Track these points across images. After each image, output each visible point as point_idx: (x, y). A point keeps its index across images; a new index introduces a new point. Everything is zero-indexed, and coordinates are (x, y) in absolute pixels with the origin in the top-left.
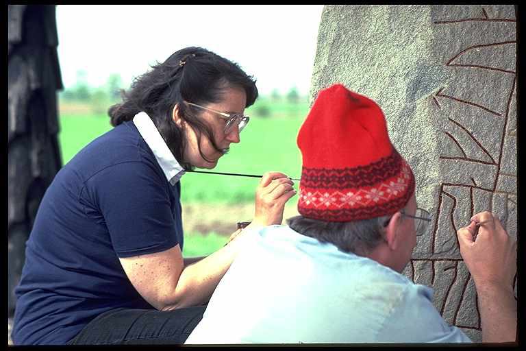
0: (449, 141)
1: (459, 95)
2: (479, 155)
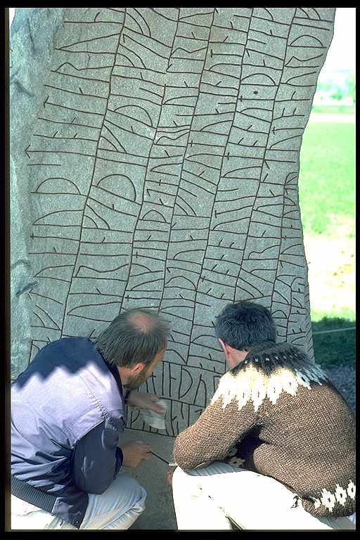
1: (41, 293)
2: (51, 325)
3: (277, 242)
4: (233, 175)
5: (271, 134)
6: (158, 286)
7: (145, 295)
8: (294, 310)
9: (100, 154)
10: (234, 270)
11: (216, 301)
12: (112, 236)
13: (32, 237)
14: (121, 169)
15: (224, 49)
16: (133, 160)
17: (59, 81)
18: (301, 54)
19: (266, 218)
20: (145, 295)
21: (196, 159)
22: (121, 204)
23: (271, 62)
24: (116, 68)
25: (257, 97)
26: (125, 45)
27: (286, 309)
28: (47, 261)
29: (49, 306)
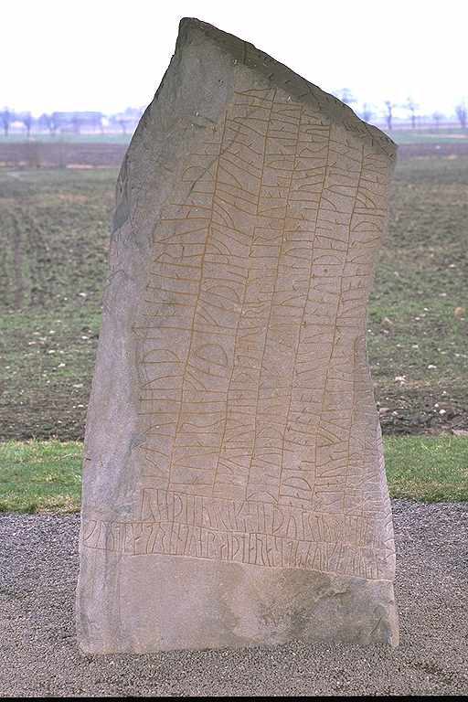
13: (141, 400)
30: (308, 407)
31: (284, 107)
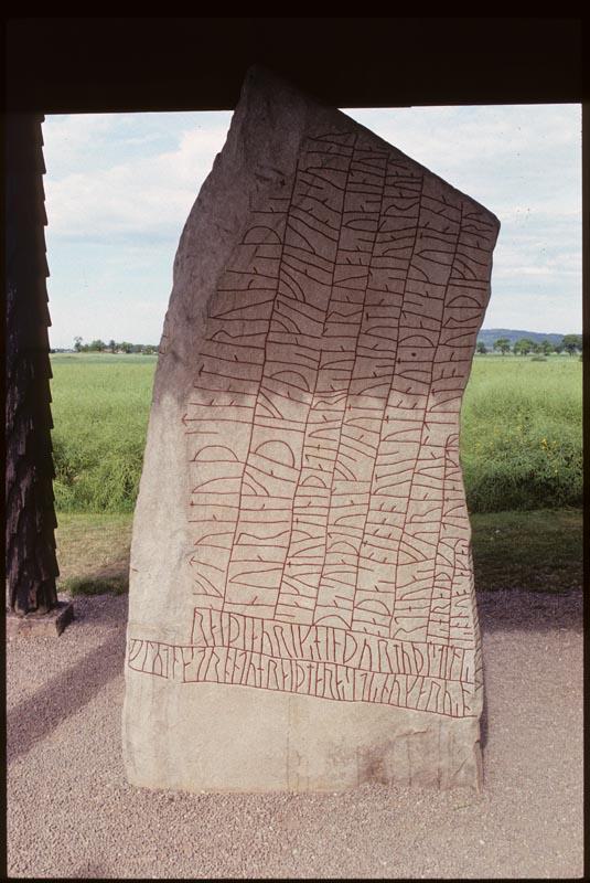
0: (196, 585)
2: (214, 593)
3: (439, 504)
4: (394, 437)
5: (431, 396)
6: (320, 551)
7: (307, 561)
8: (458, 572)
9: (257, 420)
10: (397, 533)
11: (379, 566)
12: (269, 503)
13: (192, 504)
14: (278, 435)
15: (380, 311)
16: (292, 425)
17: (213, 349)
18: (457, 314)
19: (427, 481)
20: (307, 561)
21: (354, 423)
22: (280, 471)
23: (427, 323)
24: (271, 334)
25: (415, 358)
26: (279, 310)
27: (450, 571)
28: (207, 529)
29: (209, 573)
30: (390, 518)
31: (365, 155)
